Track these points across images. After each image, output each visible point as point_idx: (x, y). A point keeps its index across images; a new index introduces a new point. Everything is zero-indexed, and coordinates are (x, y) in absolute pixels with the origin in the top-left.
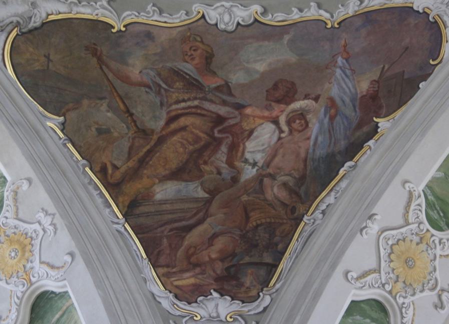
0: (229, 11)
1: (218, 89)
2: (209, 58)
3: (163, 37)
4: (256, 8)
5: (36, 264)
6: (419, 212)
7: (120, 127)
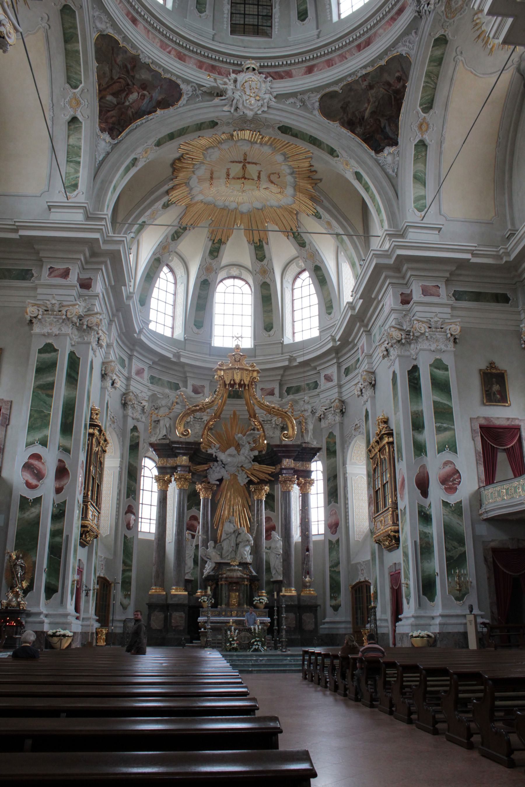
0: (145, 57)
1: (132, 76)
2: (134, 67)
4: (151, 61)
5: (79, 110)
6: (154, 144)
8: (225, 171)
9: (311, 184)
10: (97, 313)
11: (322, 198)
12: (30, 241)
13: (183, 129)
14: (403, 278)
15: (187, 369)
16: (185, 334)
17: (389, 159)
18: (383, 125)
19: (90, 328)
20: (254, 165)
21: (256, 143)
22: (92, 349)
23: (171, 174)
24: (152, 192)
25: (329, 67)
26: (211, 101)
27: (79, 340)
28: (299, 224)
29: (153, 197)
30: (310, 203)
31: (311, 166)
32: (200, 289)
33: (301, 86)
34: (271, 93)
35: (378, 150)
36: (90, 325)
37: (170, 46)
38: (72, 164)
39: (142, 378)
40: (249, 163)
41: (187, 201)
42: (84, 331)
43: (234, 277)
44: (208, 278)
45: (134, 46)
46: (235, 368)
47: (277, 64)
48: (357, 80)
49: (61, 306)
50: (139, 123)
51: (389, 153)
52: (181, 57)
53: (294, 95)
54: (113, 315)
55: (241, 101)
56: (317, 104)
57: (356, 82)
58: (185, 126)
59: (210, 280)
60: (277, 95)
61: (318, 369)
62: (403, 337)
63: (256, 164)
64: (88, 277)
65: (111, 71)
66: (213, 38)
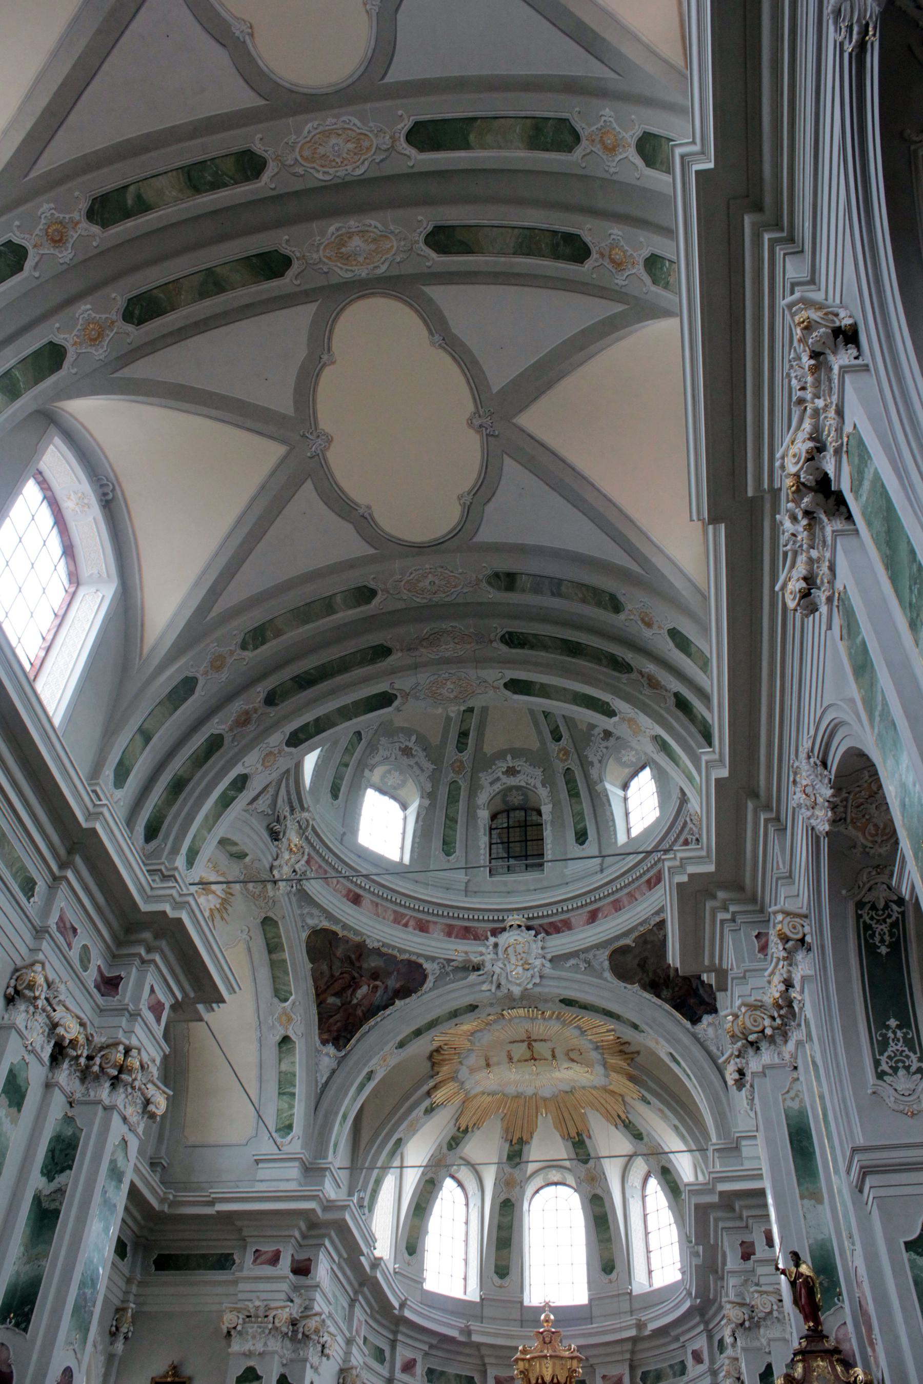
2: (360, 955)
3: (351, 943)
7: (327, 972)
8: (505, 1054)
9: (625, 1060)
10: (315, 1315)
11: (645, 1078)
12: (230, 1216)
13: (432, 1021)
14: (740, 1218)
15: (484, 1351)
16: (481, 1290)
17: (711, 1032)
18: (694, 986)
19: (307, 1336)
20: (543, 1043)
21: (537, 1018)
22: (312, 1367)
23: (429, 1069)
24: (406, 1097)
25: (616, 911)
26: (466, 978)
27: (293, 1356)
28: (628, 1107)
29: (407, 1105)
30: (631, 1085)
31: (618, 1038)
32: (500, 1214)
33: (583, 942)
34: (544, 957)
35: (695, 1020)
36: (307, 1333)
37: (406, 915)
38: (285, 1097)
39: (413, 1375)
40: (535, 1041)
41: (462, 1096)
42: (299, 1342)
43: (556, 1184)
44: (510, 1197)
45: (357, 933)
46: (546, 1357)
47: (550, 912)
48: (651, 930)
49: (267, 1308)
50: (373, 1023)
51: (709, 1024)
52: (423, 927)
53: (574, 954)
54: (356, 1292)
55: (504, 975)
56: (606, 964)
57: (650, 931)
58: (434, 1017)
59: (513, 1200)
60: (553, 957)
61: (682, 1339)
62: (746, 1317)
63: (545, 1040)
64: (307, 1257)
65: (331, 968)
66: (466, 887)
